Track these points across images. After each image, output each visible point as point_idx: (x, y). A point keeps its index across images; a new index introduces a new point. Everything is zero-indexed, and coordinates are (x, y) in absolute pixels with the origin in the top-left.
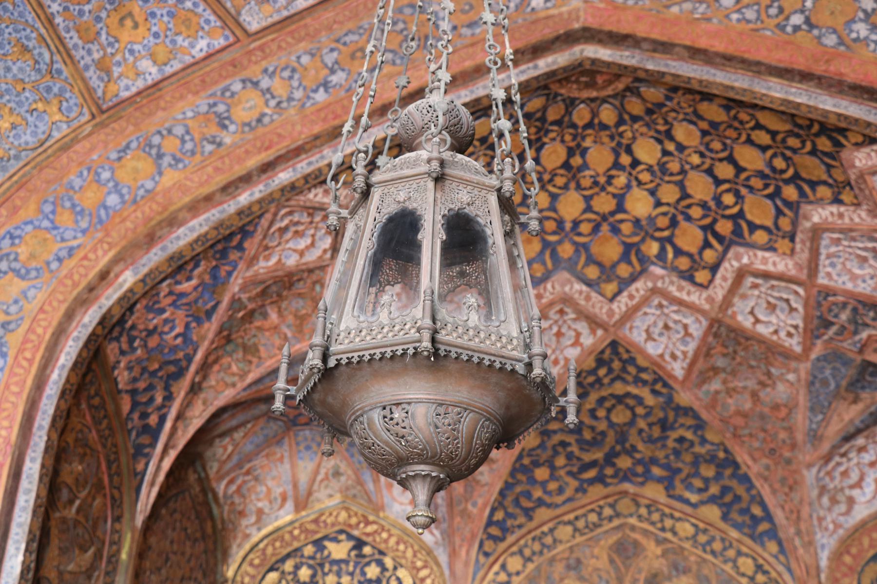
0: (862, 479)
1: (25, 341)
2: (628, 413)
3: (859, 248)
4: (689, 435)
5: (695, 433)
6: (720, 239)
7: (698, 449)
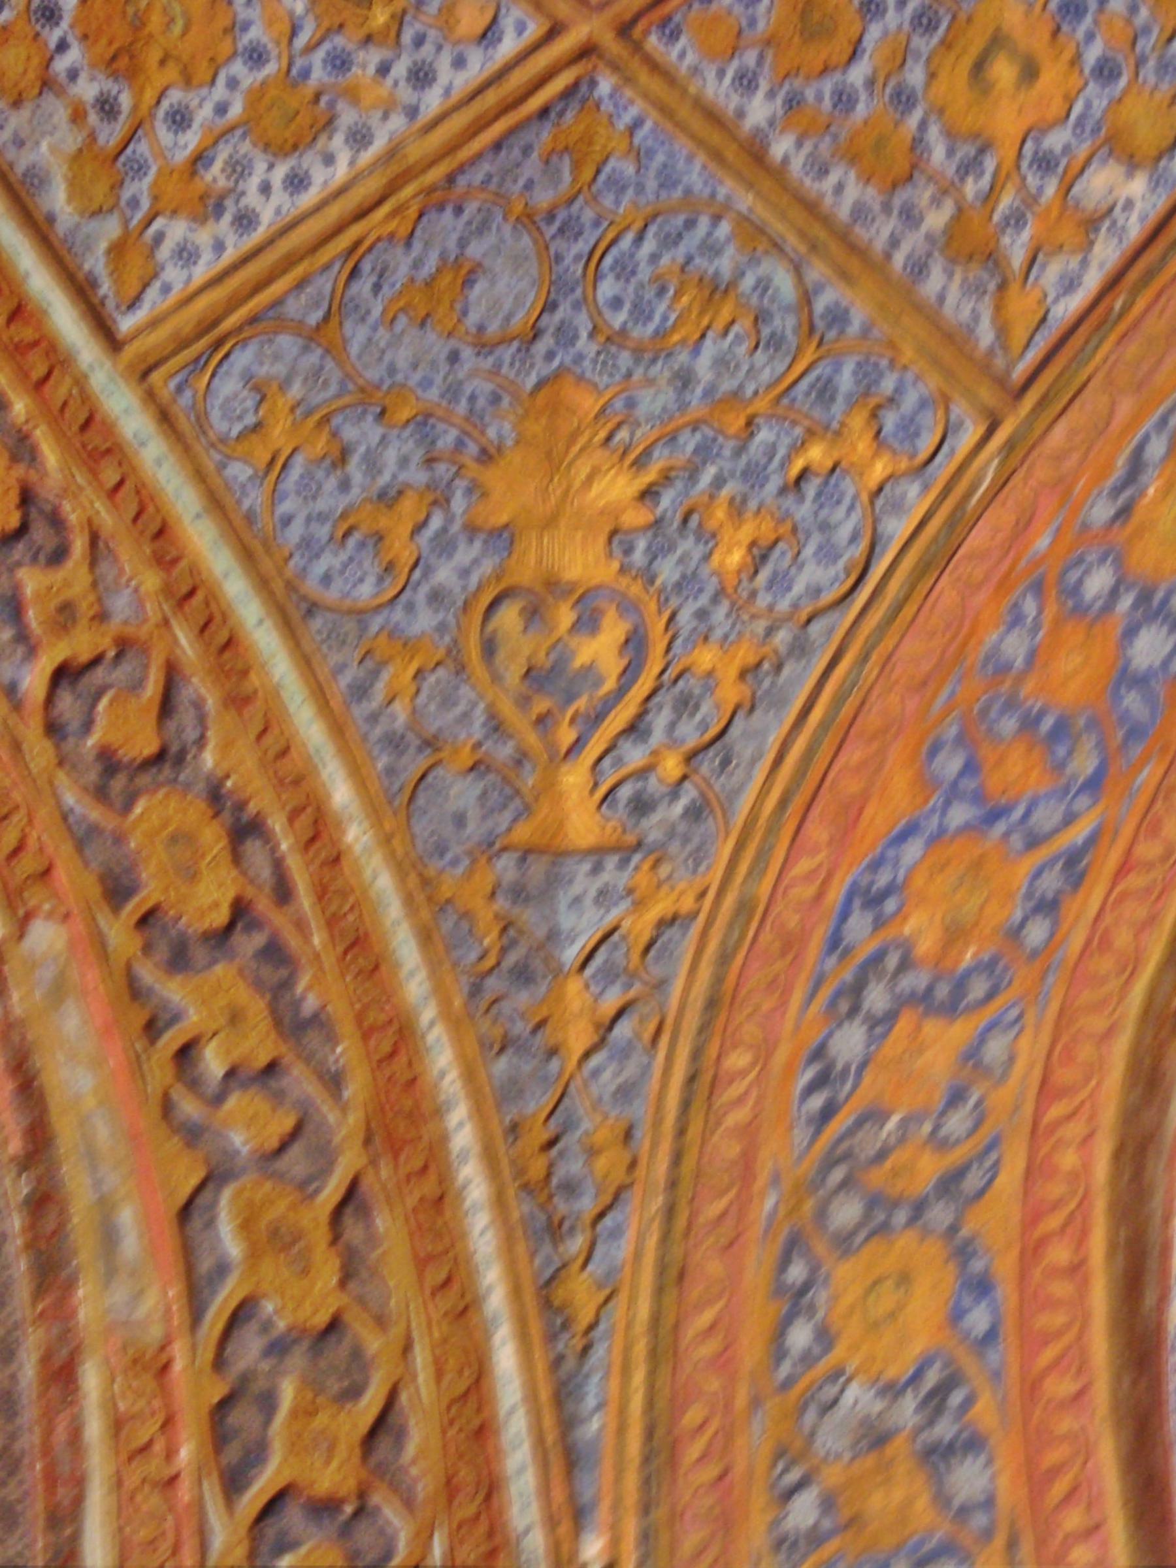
1: (1032, 1218)
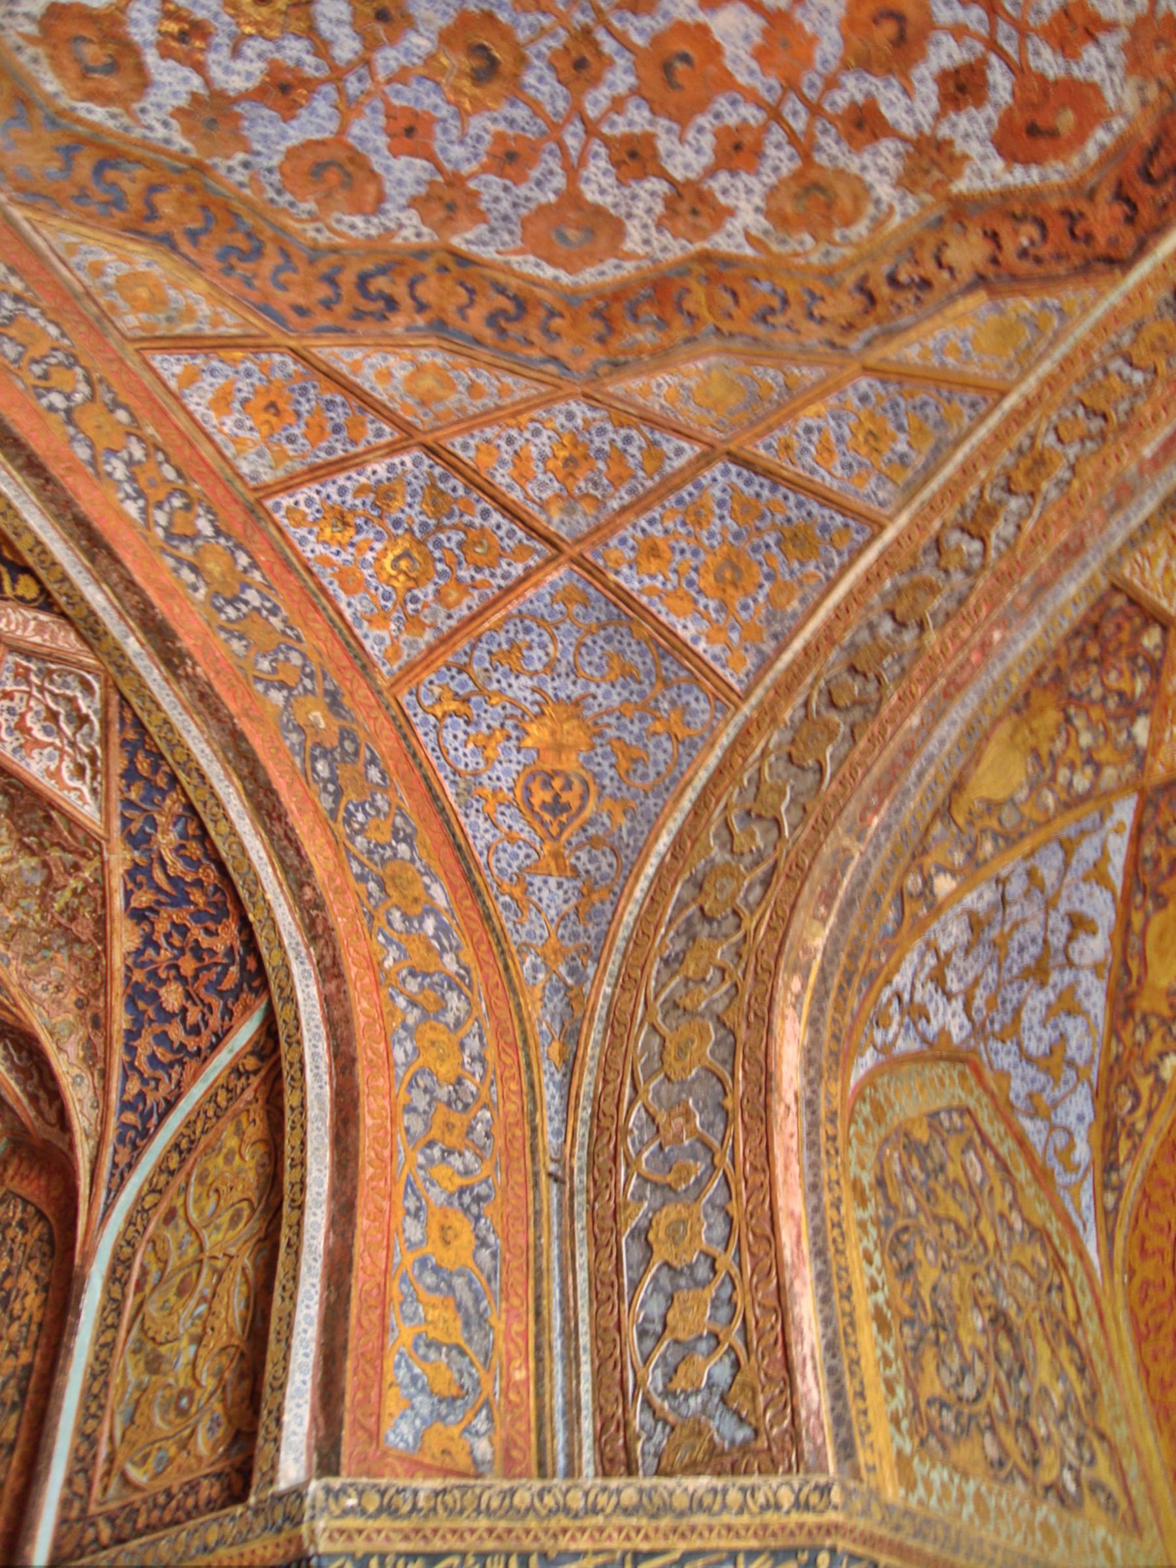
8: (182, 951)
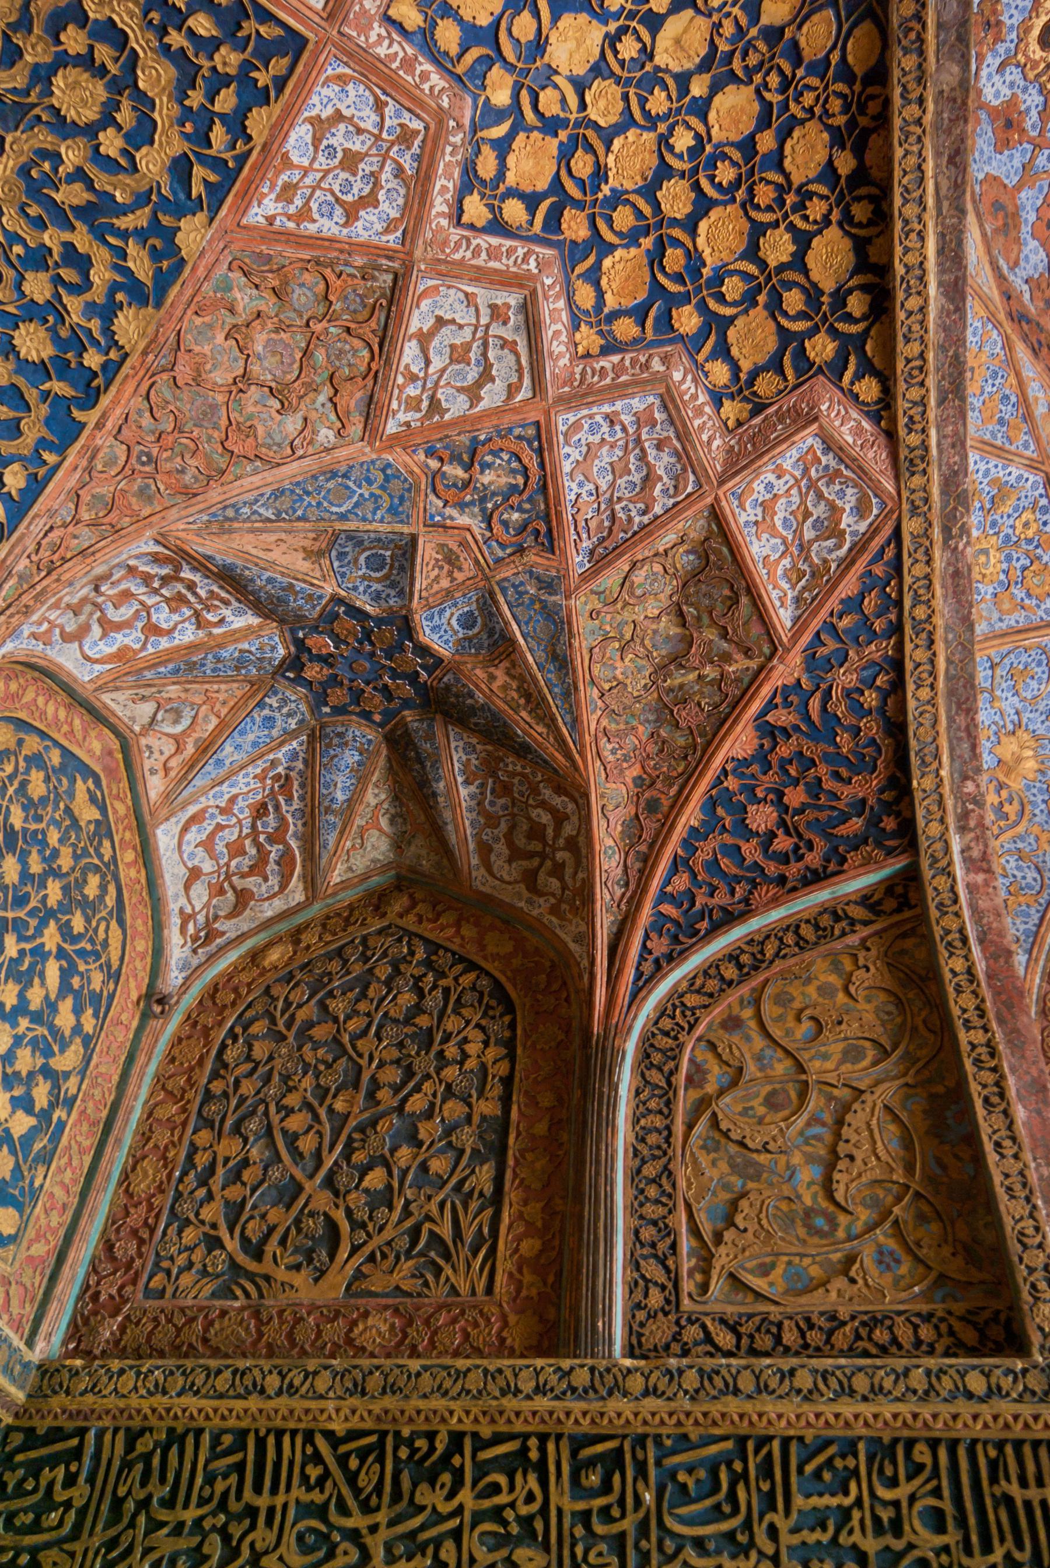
0: (119, 627)
2: (90, 114)
3: (643, 457)
4: (101, 275)
5: (114, 288)
6: (554, 221)
7: (74, 304)
8: (796, 782)
